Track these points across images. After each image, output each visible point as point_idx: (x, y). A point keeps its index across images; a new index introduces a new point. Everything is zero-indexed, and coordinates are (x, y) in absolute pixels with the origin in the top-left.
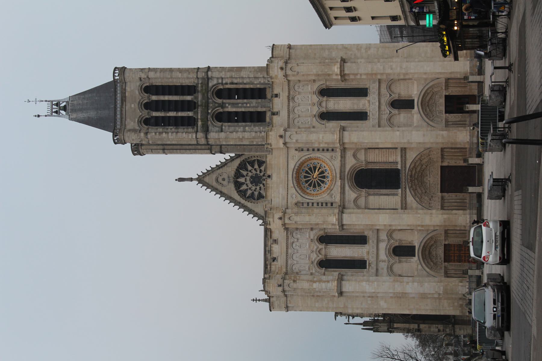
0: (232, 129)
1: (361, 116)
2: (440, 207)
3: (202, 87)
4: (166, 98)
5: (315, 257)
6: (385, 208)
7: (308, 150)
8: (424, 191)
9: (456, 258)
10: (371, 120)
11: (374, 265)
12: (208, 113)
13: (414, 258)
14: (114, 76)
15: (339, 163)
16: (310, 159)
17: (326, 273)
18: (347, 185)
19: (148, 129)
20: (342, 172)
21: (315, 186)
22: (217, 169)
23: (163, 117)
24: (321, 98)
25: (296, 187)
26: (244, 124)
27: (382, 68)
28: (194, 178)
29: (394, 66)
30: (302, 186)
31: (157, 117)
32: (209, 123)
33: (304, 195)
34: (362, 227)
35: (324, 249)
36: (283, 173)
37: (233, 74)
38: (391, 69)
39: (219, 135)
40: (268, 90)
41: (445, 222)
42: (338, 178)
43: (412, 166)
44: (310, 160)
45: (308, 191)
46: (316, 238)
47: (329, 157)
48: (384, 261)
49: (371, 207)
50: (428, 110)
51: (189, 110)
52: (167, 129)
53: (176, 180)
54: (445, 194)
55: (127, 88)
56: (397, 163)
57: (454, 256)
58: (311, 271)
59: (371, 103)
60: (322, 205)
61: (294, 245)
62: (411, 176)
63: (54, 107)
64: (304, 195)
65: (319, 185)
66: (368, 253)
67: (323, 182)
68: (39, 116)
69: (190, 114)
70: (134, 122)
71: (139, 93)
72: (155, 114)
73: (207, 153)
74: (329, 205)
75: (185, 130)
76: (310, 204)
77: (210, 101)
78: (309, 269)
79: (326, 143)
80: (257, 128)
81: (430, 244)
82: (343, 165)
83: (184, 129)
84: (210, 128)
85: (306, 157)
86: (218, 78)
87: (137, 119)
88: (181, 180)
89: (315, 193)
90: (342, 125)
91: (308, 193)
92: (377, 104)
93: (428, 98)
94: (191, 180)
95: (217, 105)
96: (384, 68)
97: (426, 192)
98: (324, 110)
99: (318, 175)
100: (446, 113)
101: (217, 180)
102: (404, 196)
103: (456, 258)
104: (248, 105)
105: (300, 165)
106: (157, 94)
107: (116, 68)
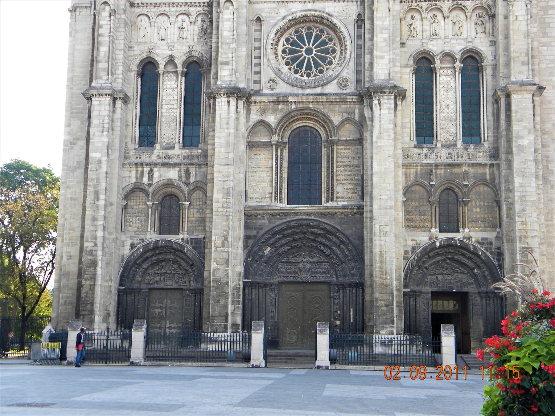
5: (161, 56)
7: (359, 37)
11: (145, 158)
24: (458, 57)
30: (292, 30)
44: (340, 40)
45: (283, 40)
46: (196, 54)
47: (344, 74)
48: (151, 177)
50: (438, 258)
57: (161, 308)
58: (135, 48)
59: (451, 150)
61: (185, 17)
74: (256, 77)
79: (371, 64)
81: (183, 263)
85: (346, 34)
89: (280, 53)
91: (279, 39)
93: (462, 259)
98: (437, 64)
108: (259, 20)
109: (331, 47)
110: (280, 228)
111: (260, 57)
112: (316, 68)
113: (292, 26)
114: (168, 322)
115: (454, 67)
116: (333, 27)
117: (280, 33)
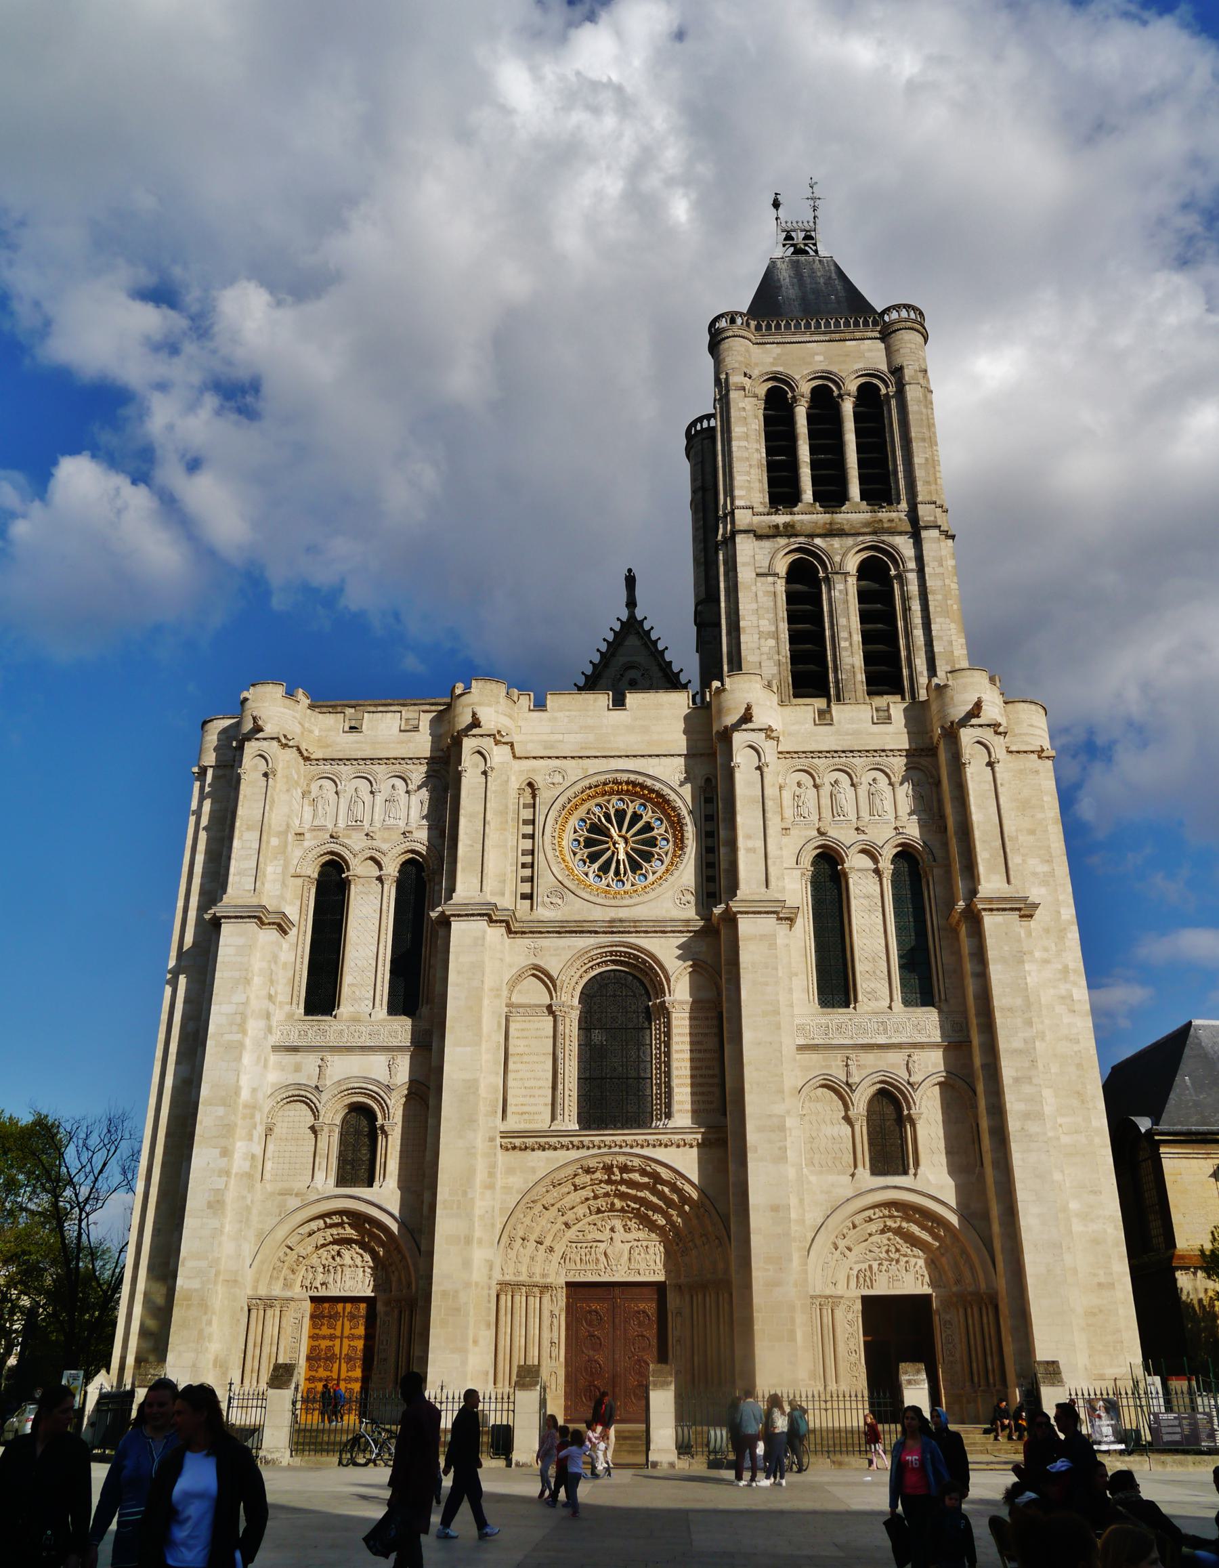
0: (767, 601)
1: (836, 982)
2: (507, 1278)
3: (891, 521)
4: (850, 438)
5: (354, 847)
6: (511, 1076)
8: (570, 1216)
9: (324, 1344)
10: (823, 1020)
12: (812, 536)
13: (332, 1180)
14: (897, 307)
15: (668, 916)
16: (677, 826)
17: (300, 881)
18: (591, 941)
19: (756, 396)
20: (637, 927)
21: (589, 843)
22: (660, 665)
23: (792, 437)
25: (586, 783)
26: (785, 636)
27: (1017, 1044)
28: (637, 611)
29: (1027, 1089)
30: (591, 804)
31: (791, 421)
32: (782, 541)
33: (558, 805)
34: (438, 988)
35: (378, 874)
36: (633, 742)
37: (939, 597)
38: (1017, 1080)
39: (744, 564)
40: (898, 698)
41: (445, 1294)
42: (611, 914)
43: (660, 1169)
49: (513, 1026)
50: (873, 1227)
51: (817, 497)
52: (758, 441)
53: (630, 570)
54: (562, 1302)
55: (866, 342)
56: (669, 1116)
57: (332, 1337)
58: (307, 835)
60: (524, 866)
61: (399, 783)
62: (624, 1169)
63: (802, 235)
64: (558, 805)
65: (593, 858)
66: (356, 1020)
67: (605, 869)
68: (776, 205)
69: (808, 495)
70: (773, 364)
71: (856, 371)
72: (801, 413)
73: (696, 595)
74: (526, 888)
75: (757, 485)
76: (528, 829)
77: (850, 541)
78: (316, 829)
80: (775, 670)
82: (660, 929)
83: (761, 481)
84: (767, 544)
86: (919, 559)
87: (780, 369)
88: (630, 581)
90: (799, 921)
91: (566, 820)
92: (881, 1040)
93: (915, 1229)
94: (631, 603)
95: (837, 559)
96: (1018, 1052)
97: (567, 1225)
99: (620, 831)
100: (866, 1300)
101: (630, 666)
102: (553, 1141)
103: (324, 1344)
104: (844, 644)
105: (659, 794)
106: (858, 417)
107: (921, 314)
108: (530, 785)
109: (660, 835)
110: (570, 1171)
111: (532, 853)
112: (634, 872)
113: (591, 797)
114: (344, 1366)
115: (877, 872)
116: (661, 803)
117: (570, 808)
